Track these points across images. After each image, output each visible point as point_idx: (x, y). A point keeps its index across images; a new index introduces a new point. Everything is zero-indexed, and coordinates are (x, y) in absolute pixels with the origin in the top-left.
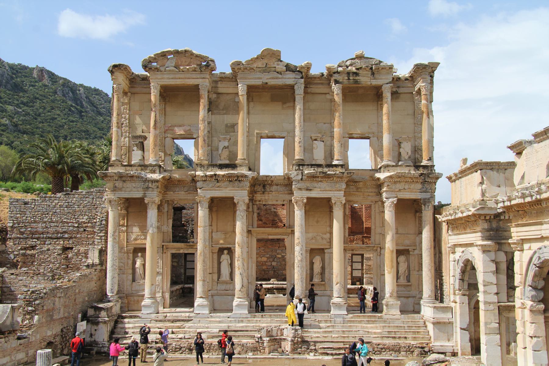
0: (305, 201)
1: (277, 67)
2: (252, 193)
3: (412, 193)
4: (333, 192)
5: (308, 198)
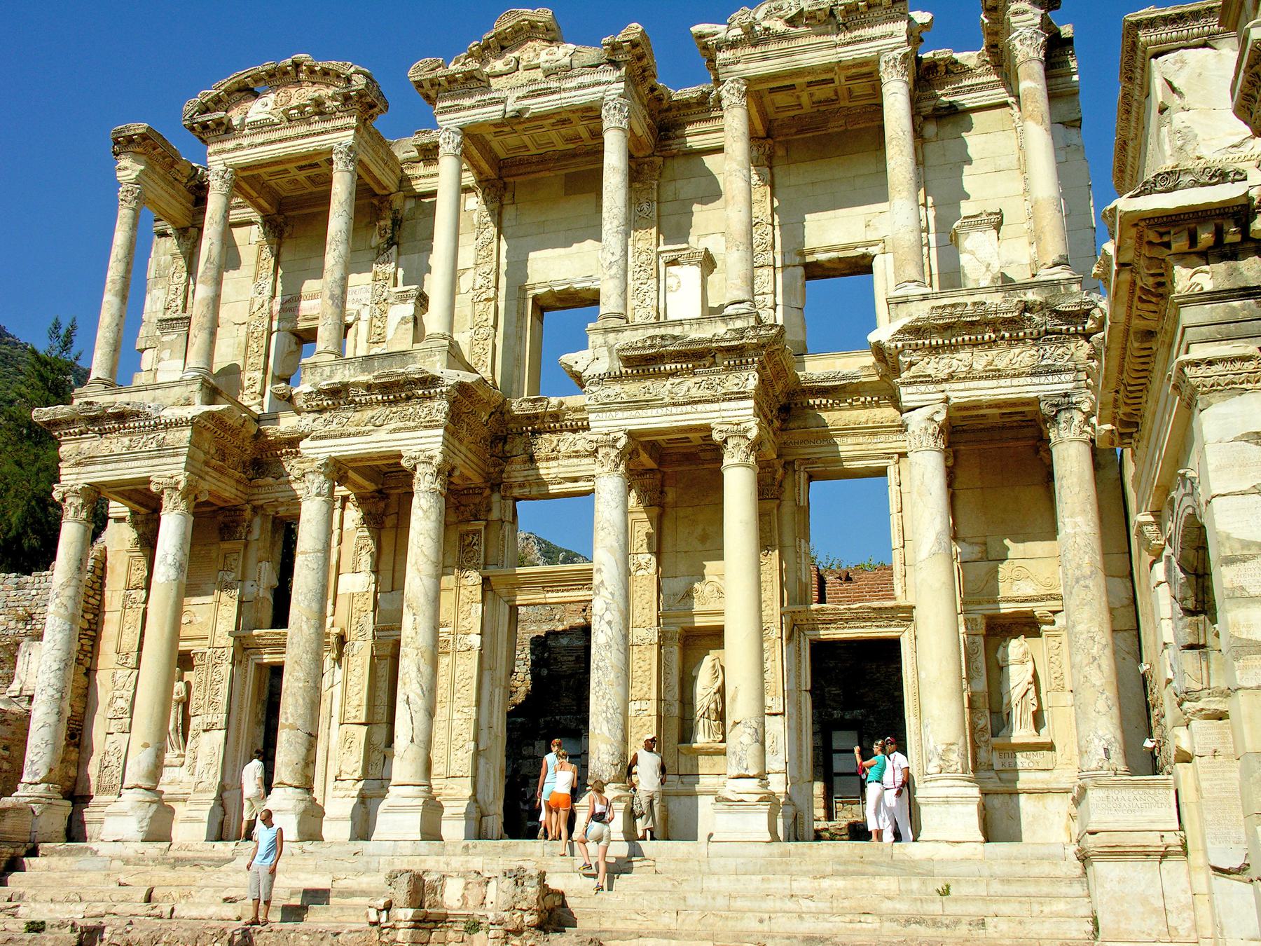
0: (621, 444)
3: (1002, 382)
4: (715, 406)
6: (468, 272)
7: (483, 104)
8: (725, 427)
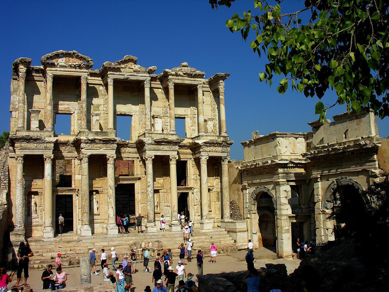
0: (153, 157)
1: (134, 68)
2: (118, 152)
3: (217, 153)
5: (155, 156)
6: (101, 105)
7: (120, 75)
8: (172, 156)
